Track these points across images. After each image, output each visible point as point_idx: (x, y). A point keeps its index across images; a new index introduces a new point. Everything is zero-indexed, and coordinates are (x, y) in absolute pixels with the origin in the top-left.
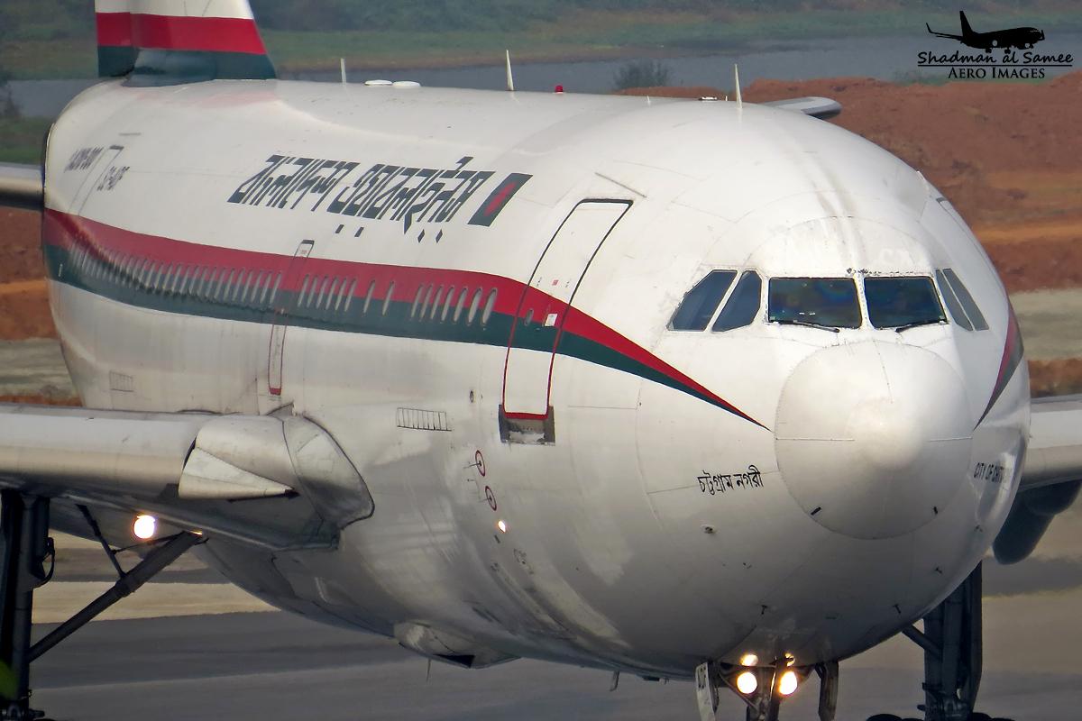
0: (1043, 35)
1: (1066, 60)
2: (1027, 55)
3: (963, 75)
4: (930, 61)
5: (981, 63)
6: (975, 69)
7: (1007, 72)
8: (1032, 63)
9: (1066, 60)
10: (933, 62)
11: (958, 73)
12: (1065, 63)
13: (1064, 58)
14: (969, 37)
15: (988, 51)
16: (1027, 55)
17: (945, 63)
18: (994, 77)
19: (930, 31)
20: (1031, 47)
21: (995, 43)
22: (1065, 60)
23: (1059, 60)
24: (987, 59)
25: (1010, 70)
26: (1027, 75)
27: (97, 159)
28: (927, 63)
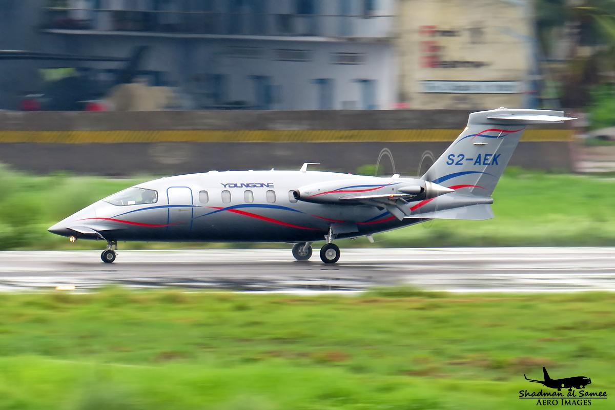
0: (590, 380)
1: (603, 395)
2: (581, 392)
3: (545, 404)
4: (526, 396)
5: (555, 397)
6: (552, 400)
7: (570, 402)
8: (584, 397)
9: (603, 395)
10: (528, 396)
11: (542, 403)
12: (603, 397)
13: (602, 394)
14: (548, 382)
15: (559, 390)
16: (581, 392)
17: (534, 397)
18: (562, 404)
19: (526, 379)
20: (584, 387)
21: (563, 385)
22: (603, 395)
23: (599, 395)
24: (559, 394)
25: (572, 400)
26: (581, 403)
27: (378, 212)
28: (524, 397)
